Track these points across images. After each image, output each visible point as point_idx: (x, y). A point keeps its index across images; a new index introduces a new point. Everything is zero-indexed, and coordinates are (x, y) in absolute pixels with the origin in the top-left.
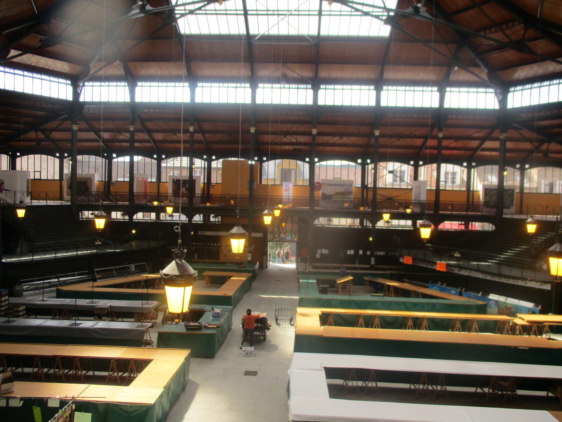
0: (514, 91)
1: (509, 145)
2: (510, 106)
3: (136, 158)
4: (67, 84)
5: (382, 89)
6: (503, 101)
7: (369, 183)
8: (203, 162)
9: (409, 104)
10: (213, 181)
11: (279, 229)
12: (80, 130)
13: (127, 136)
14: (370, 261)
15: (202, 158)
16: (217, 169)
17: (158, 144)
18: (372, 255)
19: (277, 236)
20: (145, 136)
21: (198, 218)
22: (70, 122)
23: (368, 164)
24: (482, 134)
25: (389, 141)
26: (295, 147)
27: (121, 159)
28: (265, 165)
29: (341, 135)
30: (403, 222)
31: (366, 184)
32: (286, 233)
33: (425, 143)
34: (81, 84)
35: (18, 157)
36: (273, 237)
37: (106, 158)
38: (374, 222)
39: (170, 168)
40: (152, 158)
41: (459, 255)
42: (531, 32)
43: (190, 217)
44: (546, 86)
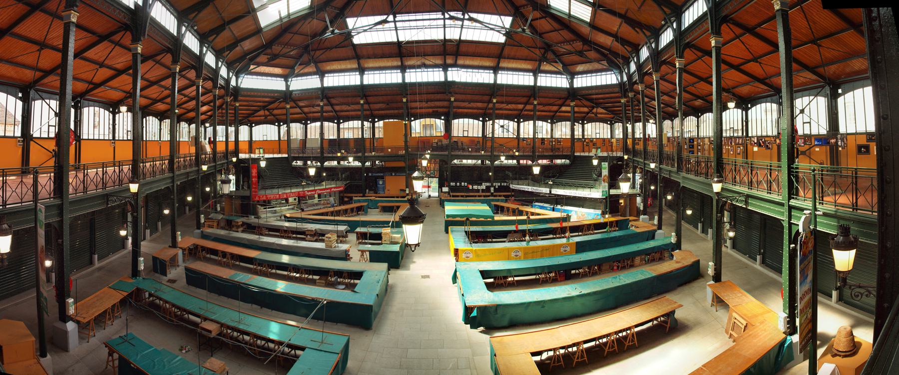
0: (577, 78)
1: (576, 109)
2: (575, 86)
3: (326, 124)
6: (571, 83)
7: (488, 133)
9: (515, 83)
10: (377, 136)
12: (291, 108)
13: (319, 109)
14: (490, 190)
15: (368, 121)
16: (379, 127)
17: (338, 113)
18: (492, 186)
20: (329, 108)
21: (368, 164)
22: (285, 103)
23: (487, 121)
24: (560, 102)
25: (504, 106)
26: (434, 109)
27: (313, 124)
28: (413, 123)
29: (470, 102)
30: (510, 162)
32: (430, 170)
33: (524, 107)
35: (377, 122)
37: (303, 124)
38: (492, 162)
39: (346, 128)
40: (334, 122)
41: (552, 183)
42: (586, 47)
43: (363, 163)
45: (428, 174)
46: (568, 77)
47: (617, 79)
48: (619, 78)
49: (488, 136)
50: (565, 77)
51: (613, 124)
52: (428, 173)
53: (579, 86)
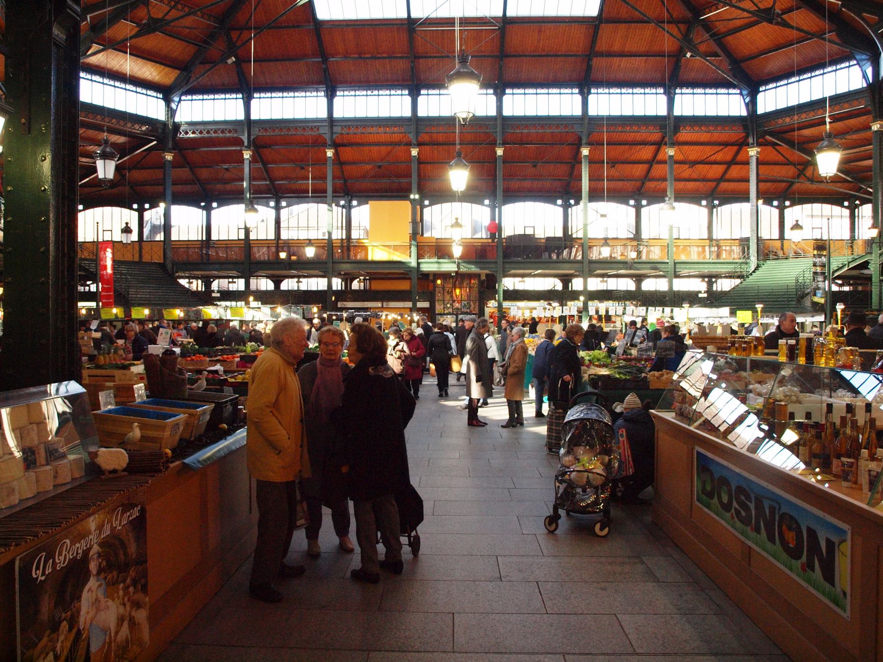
2: (760, 110)
4: (157, 97)
5: (589, 93)
6: (752, 105)
8: (340, 209)
11: (452, 296)
19: (449, 305)
23: (570, 206)
28: (426, 211)
31: (570, 233)
32: (461, 300)
34: (176, 99)
36: (444, 308)
37: (203, 208)
44: (807, 79)
45: (457, 309)
46: (745, 92)
47: (865, 76)
48: (869, 71)
49: (574, 236)
50: (738, 91)
51: (857, 206)
52: (457, 305)
53: (770, 108)
